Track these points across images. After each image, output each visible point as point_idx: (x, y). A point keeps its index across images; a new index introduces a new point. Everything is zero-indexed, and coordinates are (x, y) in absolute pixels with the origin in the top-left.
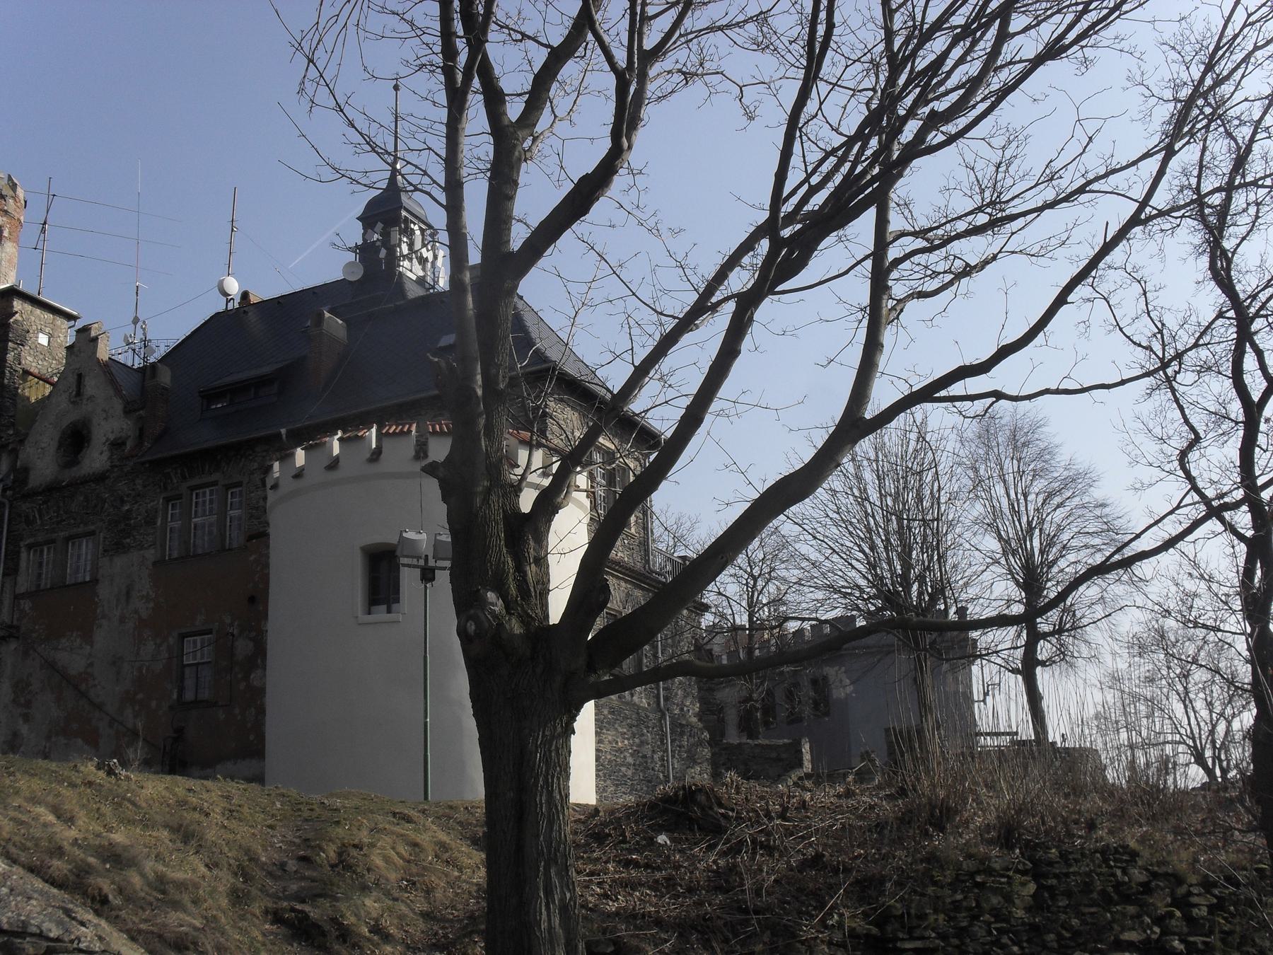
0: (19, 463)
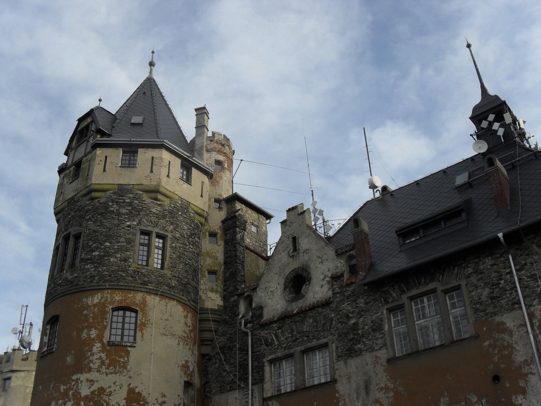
0: (254, 305)
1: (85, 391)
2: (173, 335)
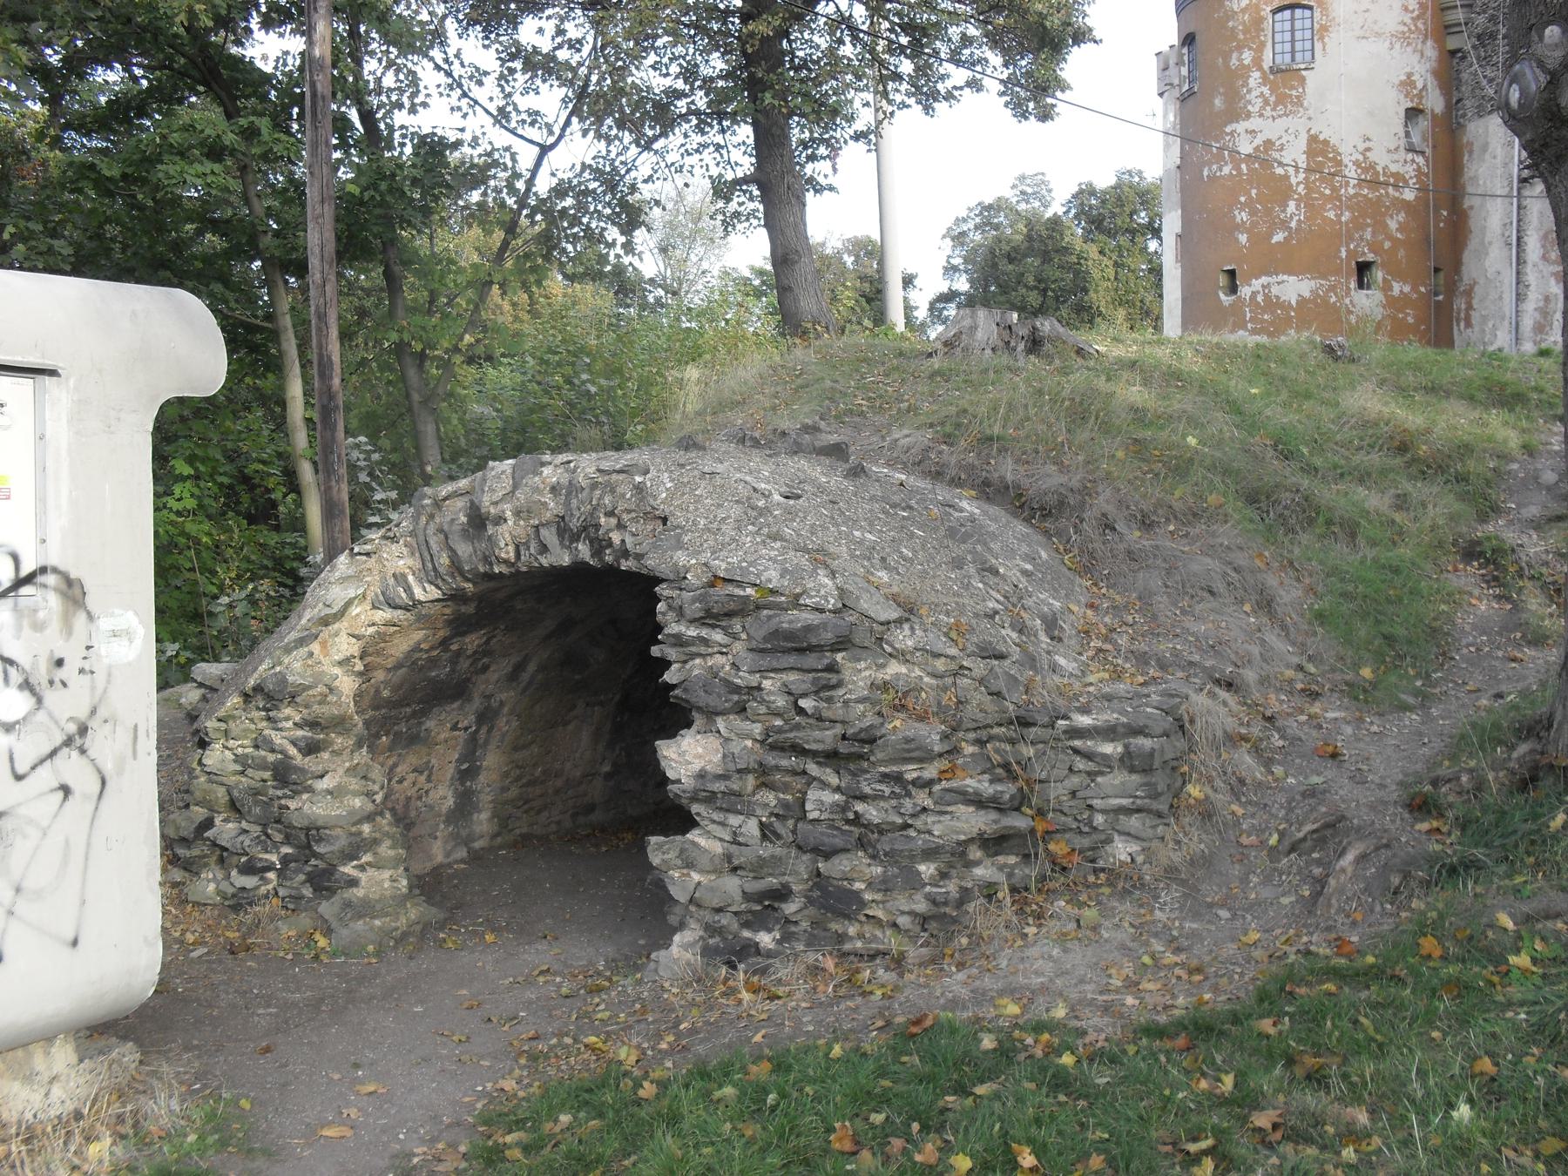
1: (1246, 148)
2: (1378, 35)
